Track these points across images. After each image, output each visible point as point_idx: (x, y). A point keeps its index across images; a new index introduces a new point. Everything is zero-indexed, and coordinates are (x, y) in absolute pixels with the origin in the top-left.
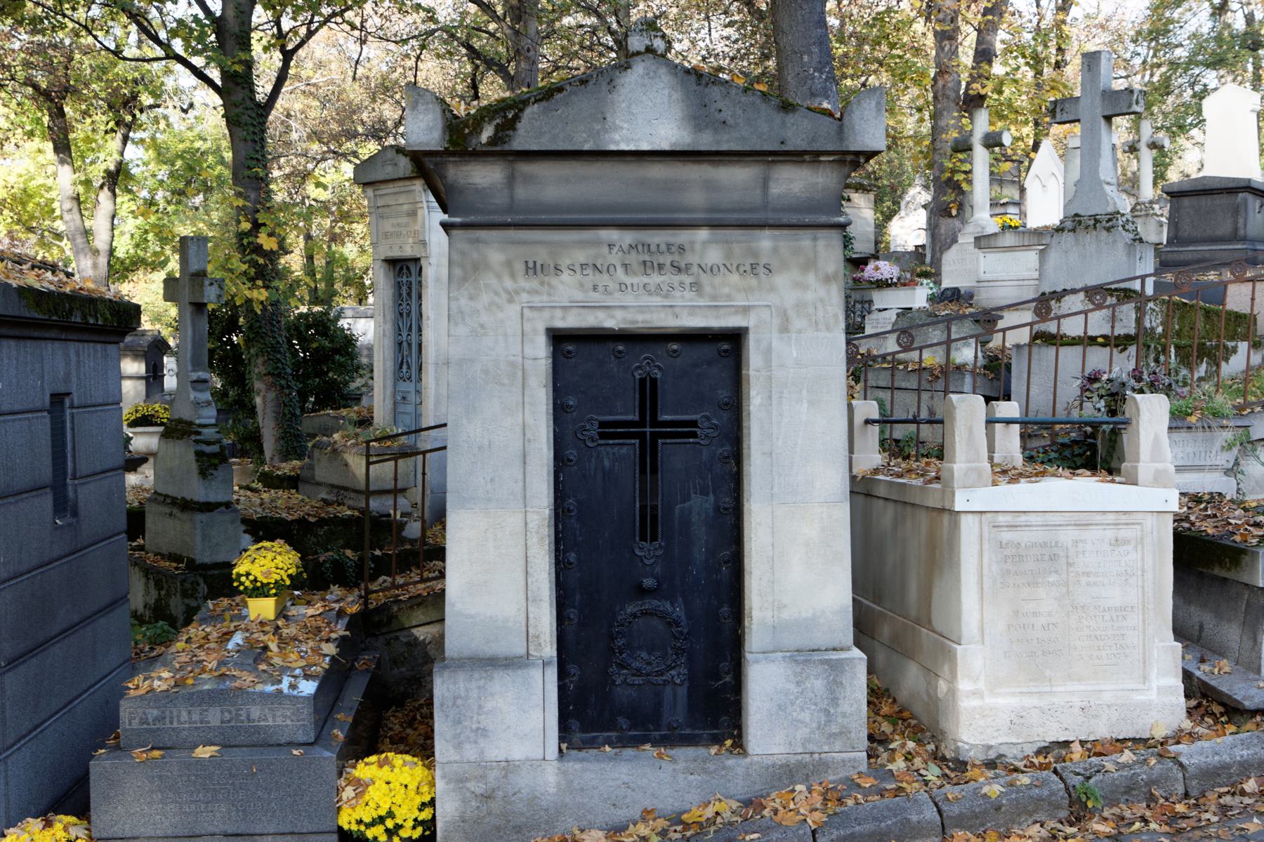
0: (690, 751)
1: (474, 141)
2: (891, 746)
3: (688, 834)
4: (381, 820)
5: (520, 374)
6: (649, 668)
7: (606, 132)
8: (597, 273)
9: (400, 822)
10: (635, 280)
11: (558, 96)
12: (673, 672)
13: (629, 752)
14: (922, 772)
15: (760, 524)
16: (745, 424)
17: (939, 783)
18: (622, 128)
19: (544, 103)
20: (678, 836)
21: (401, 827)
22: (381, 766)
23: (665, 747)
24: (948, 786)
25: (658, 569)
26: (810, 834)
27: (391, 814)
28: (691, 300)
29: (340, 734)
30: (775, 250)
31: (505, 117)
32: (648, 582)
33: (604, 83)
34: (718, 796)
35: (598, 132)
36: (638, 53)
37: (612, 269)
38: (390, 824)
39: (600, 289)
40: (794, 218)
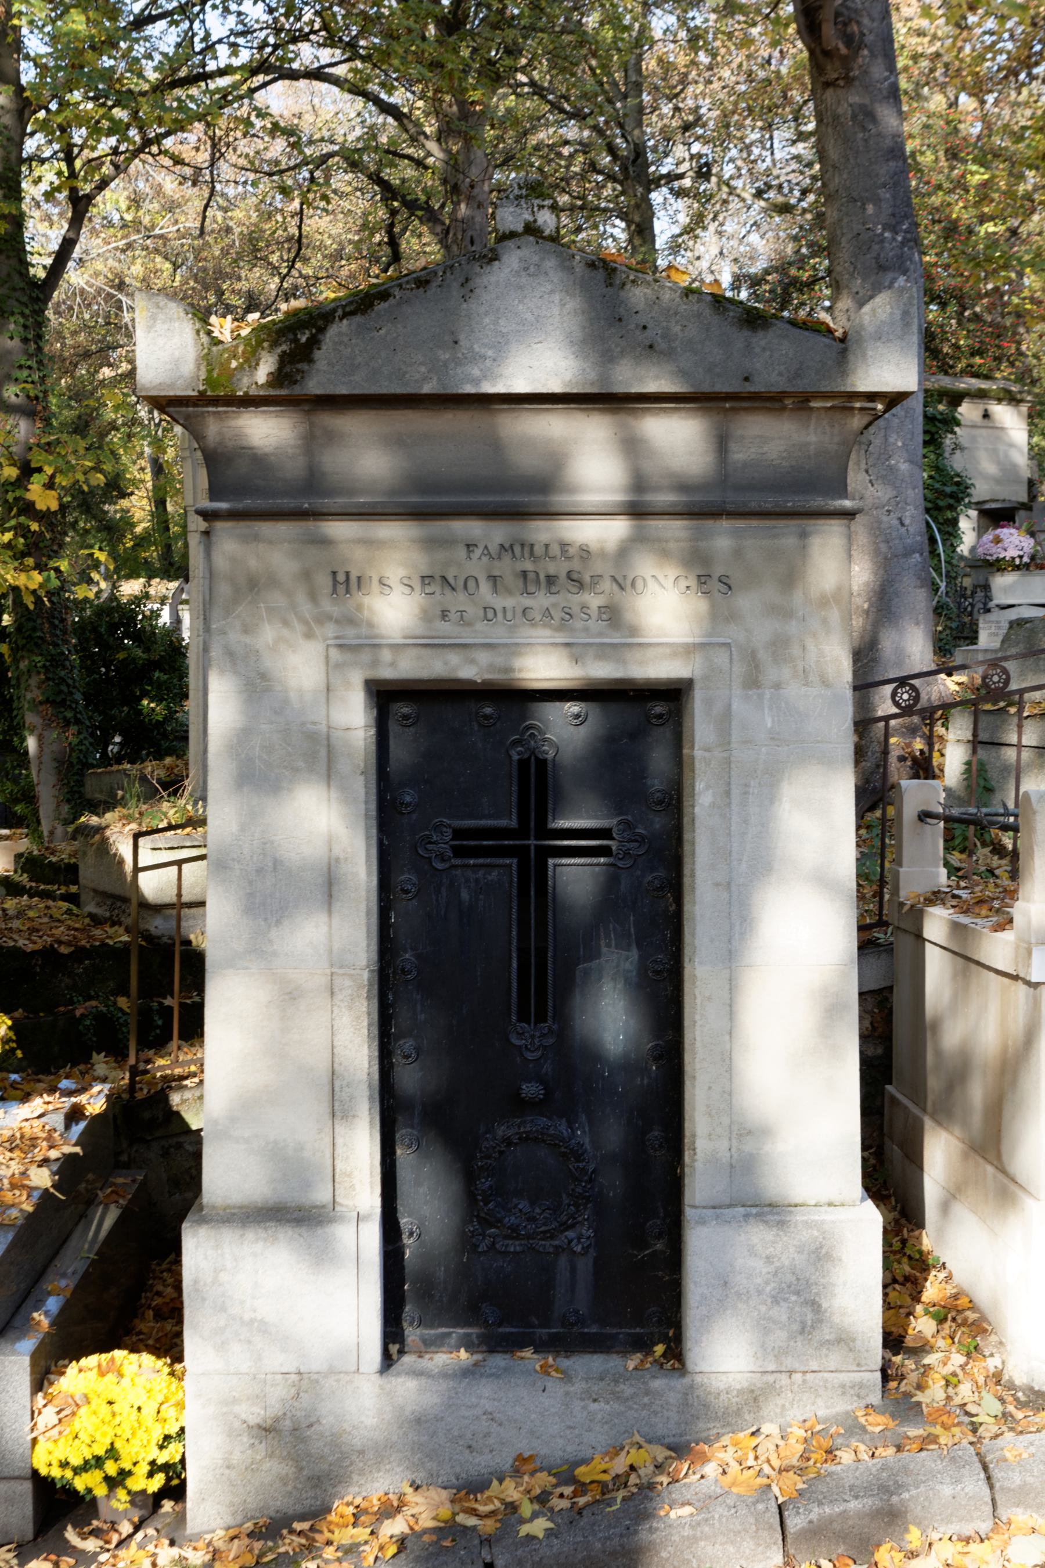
0: (596, 1362)
1: (246, 381)
2: (926, 1361)
3: (582, 1501)
4: (98, 1462)
5: (323, 752)
6: (531, 1227)
7: (459, 363)
8: (448, 591)
9: (127, 1466)
10: (509, 602)
11: (381, 307)
12: (570, 1234)
13: (499, 1360)
14: (971, 1408)
15: (709, 999)
16: (687, 836)
17: (994, 1429)
18: (484, 357)
19: (358, 319)
20: (565, 1504)
21: (130, 1473)
22: (102, 1373)
23: (557, 1354)
24: (1009, 1436)
25: (547, 1067)
26: (776, 1510)
27: (112, 1453)
28: (600, 635)
29: (42, 1319)
30: (738, 553)
31: (296, 340)
32: (530, 1089)
33: (456, 285)
34: (637, 1438)
35: (445, 364)
36: (512, 235)
37: (471, 584)
38: (111, 1468)
39: (453, 616)
40: (769, 501)
